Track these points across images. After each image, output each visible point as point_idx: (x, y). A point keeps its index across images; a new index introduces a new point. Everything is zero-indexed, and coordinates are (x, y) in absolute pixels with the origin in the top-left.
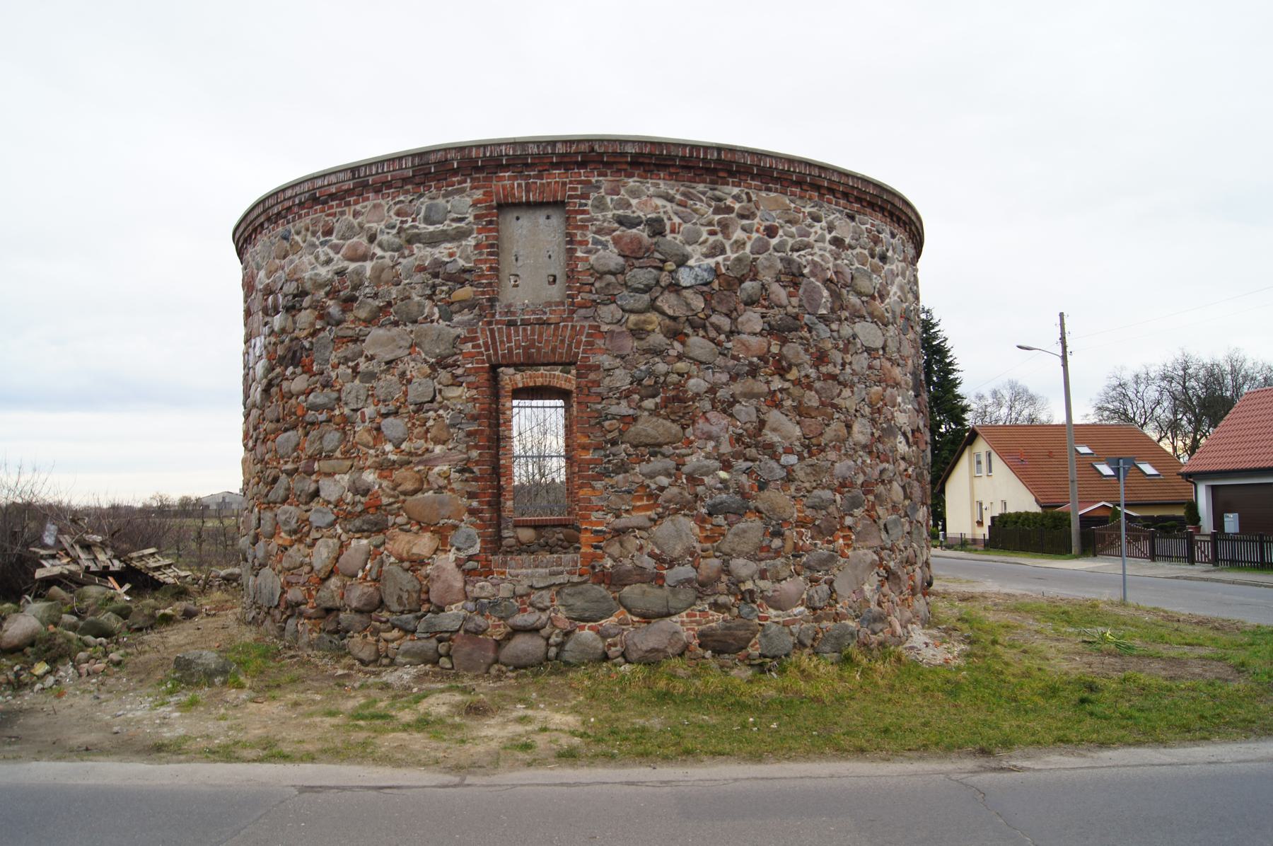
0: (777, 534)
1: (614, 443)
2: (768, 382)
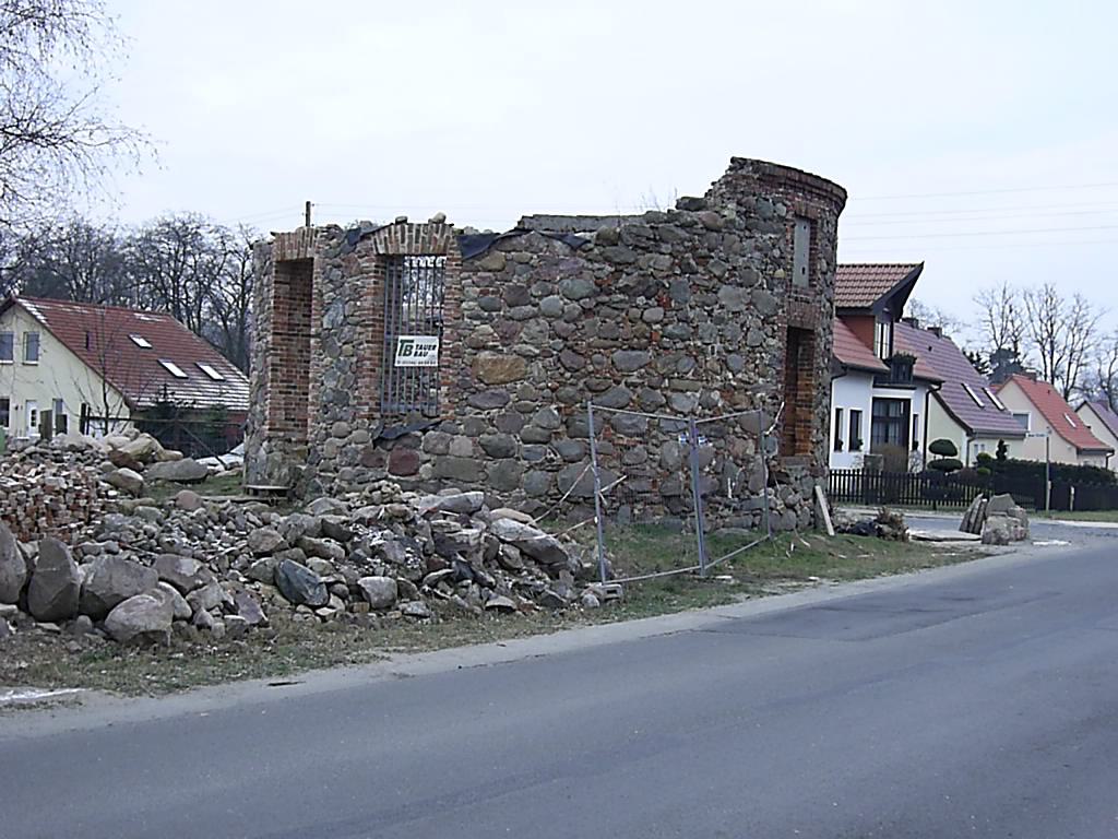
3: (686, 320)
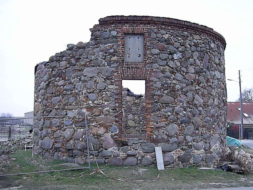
1: (156, 102)
2: (195, 87)
3: (71, 83)
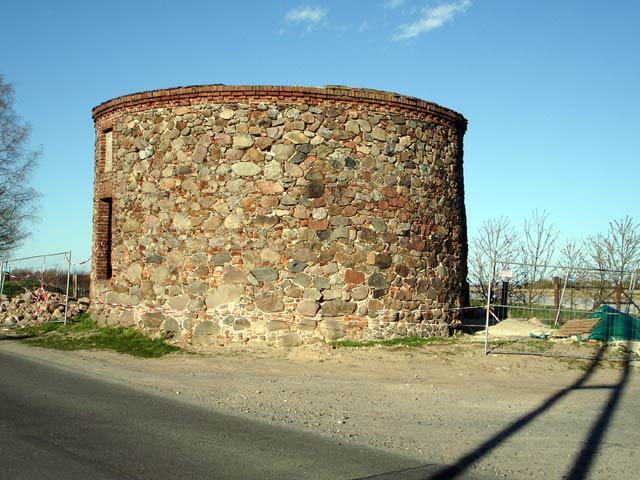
0: (175, 272)
